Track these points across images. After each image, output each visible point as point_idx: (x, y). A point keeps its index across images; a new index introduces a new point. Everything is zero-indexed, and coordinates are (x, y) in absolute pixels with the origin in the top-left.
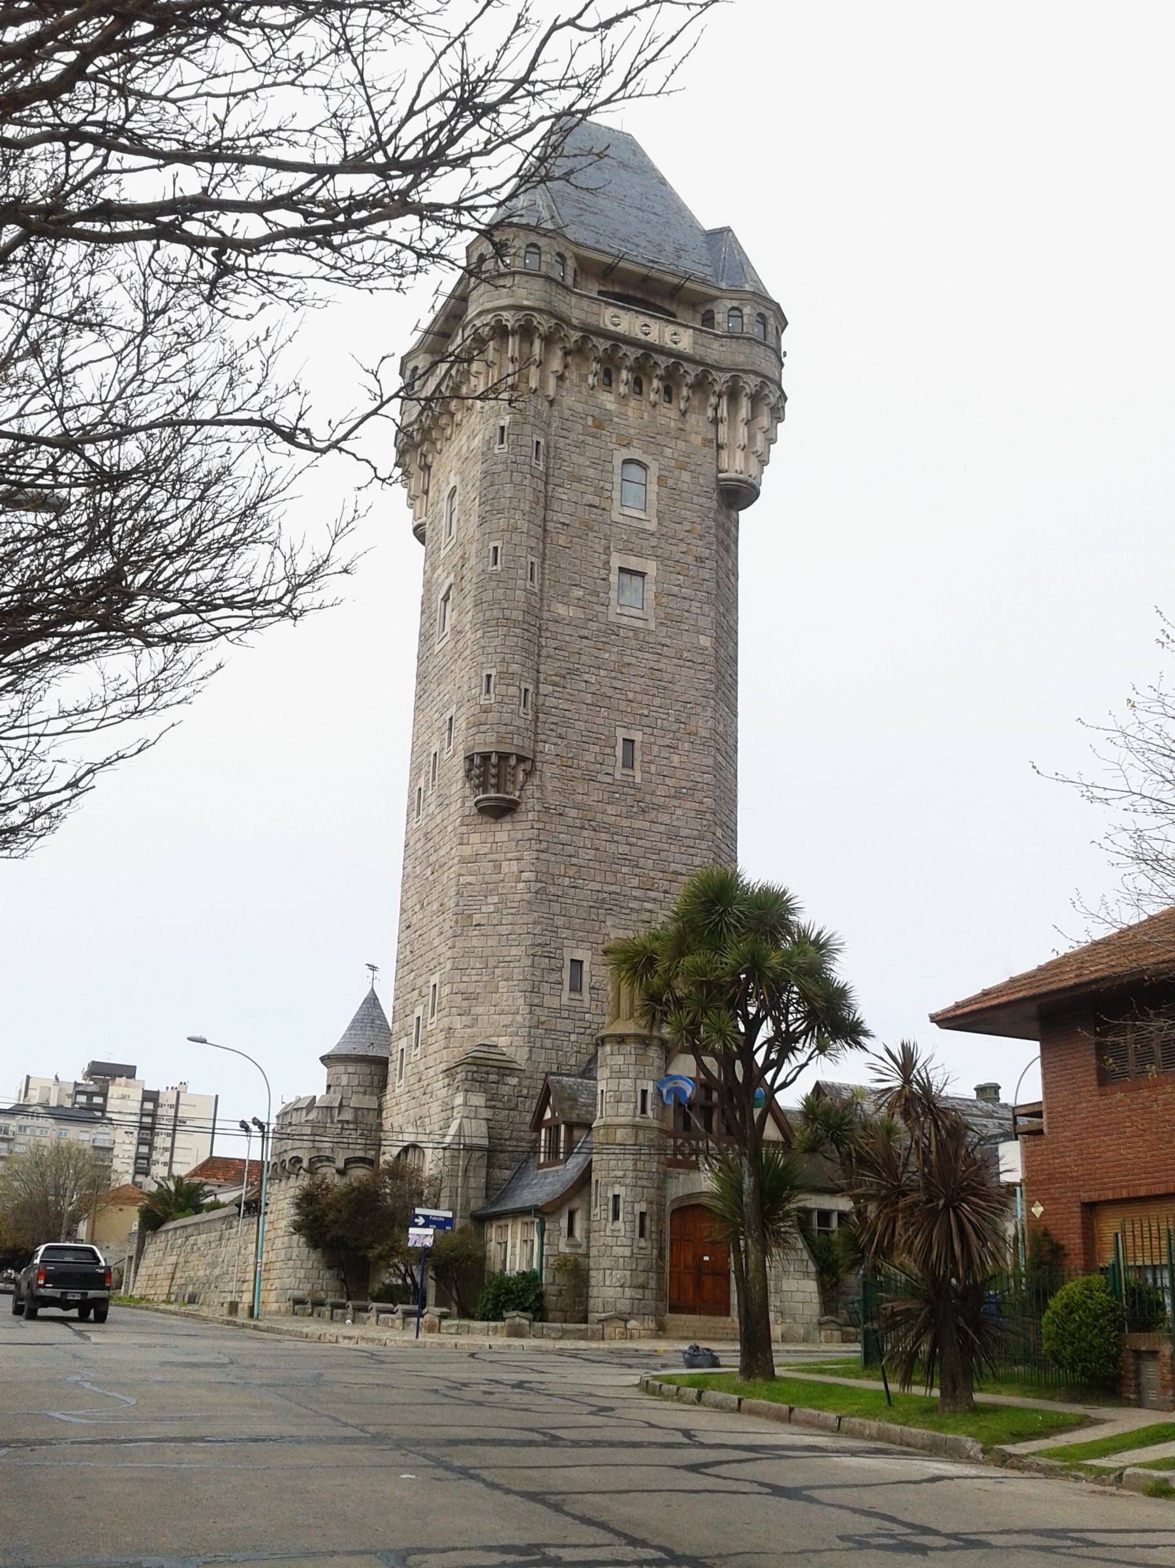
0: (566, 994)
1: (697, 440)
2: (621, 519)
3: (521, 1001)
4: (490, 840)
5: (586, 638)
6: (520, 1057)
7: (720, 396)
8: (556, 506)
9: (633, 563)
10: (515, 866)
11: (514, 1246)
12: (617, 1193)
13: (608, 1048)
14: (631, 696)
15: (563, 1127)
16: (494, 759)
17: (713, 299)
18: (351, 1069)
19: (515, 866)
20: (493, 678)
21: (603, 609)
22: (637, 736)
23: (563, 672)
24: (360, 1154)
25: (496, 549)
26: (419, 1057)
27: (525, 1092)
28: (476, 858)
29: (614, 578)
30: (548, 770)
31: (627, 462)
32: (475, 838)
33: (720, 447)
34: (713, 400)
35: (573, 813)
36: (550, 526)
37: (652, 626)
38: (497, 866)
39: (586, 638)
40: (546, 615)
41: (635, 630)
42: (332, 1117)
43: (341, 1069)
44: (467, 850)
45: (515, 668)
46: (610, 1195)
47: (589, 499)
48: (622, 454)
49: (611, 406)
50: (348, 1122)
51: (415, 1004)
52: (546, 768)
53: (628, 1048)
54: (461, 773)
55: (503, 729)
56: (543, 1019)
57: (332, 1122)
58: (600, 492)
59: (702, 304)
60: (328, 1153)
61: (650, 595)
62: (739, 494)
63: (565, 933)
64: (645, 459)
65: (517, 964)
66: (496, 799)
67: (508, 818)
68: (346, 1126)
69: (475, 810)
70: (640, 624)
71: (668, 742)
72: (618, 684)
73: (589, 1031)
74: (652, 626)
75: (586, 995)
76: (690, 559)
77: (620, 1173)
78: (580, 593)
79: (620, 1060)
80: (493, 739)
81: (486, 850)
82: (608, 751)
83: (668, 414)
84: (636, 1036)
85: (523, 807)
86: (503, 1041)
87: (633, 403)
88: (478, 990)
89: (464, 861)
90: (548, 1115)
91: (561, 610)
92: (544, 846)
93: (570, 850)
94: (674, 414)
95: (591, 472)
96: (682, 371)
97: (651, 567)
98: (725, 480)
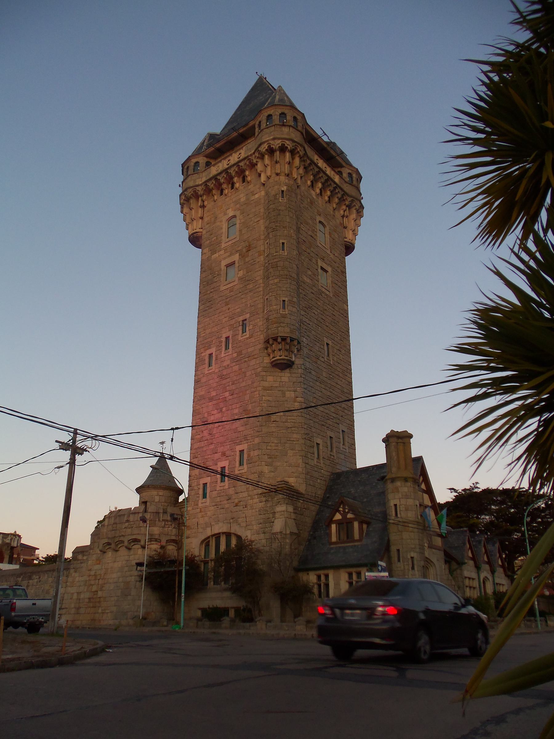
0: (316, 460)
1: (338, 221)
2: (320, 245)
4: (279, 380)
6: (302, 489)
7: (347, 206)
8: (301, 231)
9: (325, 266)
10: (293, 394)
12: (412, 556)
13: (398, 484)
15: (356, 524)
16: (288, 340)
17: (342, 166)
18: (161, 493)
19: (293, 394)
20: (286, 302)
21: (316, 282)
22: (330, 343)
24: (174, 538)
26: (227, 487)
28: (270, 388)
29: (319, 270)
30: (305, 351)
31: (320, 222)
32: (270, 378)
33: (345, 228)
34: (344, 207)
35: (313, 373)
37: (331, 295)
38: (284, 393)
40: (301, 279)
41: (327, 295)
43: (154, 492)
44: (266, 384)
45: (295, 300)
46: (409, 557)
48: (319, 218)
49: (315, 197)
50: (167, 521)
51: (218, 460)
52: (304, 349)
53: (409, 484)
54: (261, 346)
57: (159, 520)
58: (313, 231)
60: (157, 537)
61: (329, 281)
62: (349, 249)
66: (287, 360)
67: (288, 370)
68: (166, 523)
69: (269, 365)
70: (328, 293)
71: (338, 348)
72: (324, 318)
73: (323, 479)
74: (331, 295)
75: (322, 461)
76: (340, 271)
77: (413, 546)
78: (310, 273)
79: (406, 489)
80: (288, 330)
81: (277, 384)
82: (322, 347)
83: (330, 208)
84: (413, 478)
85: (295, 366)
86: (292, 481)
87: (320, 198)
88: (277, 454)
89: (265, 389)
90: (338, 517)
91: (305, 279)
92: (306, 386)
93: (313, 390)
94: (332, 209)
95: (310, 222)
97: (329, 269)
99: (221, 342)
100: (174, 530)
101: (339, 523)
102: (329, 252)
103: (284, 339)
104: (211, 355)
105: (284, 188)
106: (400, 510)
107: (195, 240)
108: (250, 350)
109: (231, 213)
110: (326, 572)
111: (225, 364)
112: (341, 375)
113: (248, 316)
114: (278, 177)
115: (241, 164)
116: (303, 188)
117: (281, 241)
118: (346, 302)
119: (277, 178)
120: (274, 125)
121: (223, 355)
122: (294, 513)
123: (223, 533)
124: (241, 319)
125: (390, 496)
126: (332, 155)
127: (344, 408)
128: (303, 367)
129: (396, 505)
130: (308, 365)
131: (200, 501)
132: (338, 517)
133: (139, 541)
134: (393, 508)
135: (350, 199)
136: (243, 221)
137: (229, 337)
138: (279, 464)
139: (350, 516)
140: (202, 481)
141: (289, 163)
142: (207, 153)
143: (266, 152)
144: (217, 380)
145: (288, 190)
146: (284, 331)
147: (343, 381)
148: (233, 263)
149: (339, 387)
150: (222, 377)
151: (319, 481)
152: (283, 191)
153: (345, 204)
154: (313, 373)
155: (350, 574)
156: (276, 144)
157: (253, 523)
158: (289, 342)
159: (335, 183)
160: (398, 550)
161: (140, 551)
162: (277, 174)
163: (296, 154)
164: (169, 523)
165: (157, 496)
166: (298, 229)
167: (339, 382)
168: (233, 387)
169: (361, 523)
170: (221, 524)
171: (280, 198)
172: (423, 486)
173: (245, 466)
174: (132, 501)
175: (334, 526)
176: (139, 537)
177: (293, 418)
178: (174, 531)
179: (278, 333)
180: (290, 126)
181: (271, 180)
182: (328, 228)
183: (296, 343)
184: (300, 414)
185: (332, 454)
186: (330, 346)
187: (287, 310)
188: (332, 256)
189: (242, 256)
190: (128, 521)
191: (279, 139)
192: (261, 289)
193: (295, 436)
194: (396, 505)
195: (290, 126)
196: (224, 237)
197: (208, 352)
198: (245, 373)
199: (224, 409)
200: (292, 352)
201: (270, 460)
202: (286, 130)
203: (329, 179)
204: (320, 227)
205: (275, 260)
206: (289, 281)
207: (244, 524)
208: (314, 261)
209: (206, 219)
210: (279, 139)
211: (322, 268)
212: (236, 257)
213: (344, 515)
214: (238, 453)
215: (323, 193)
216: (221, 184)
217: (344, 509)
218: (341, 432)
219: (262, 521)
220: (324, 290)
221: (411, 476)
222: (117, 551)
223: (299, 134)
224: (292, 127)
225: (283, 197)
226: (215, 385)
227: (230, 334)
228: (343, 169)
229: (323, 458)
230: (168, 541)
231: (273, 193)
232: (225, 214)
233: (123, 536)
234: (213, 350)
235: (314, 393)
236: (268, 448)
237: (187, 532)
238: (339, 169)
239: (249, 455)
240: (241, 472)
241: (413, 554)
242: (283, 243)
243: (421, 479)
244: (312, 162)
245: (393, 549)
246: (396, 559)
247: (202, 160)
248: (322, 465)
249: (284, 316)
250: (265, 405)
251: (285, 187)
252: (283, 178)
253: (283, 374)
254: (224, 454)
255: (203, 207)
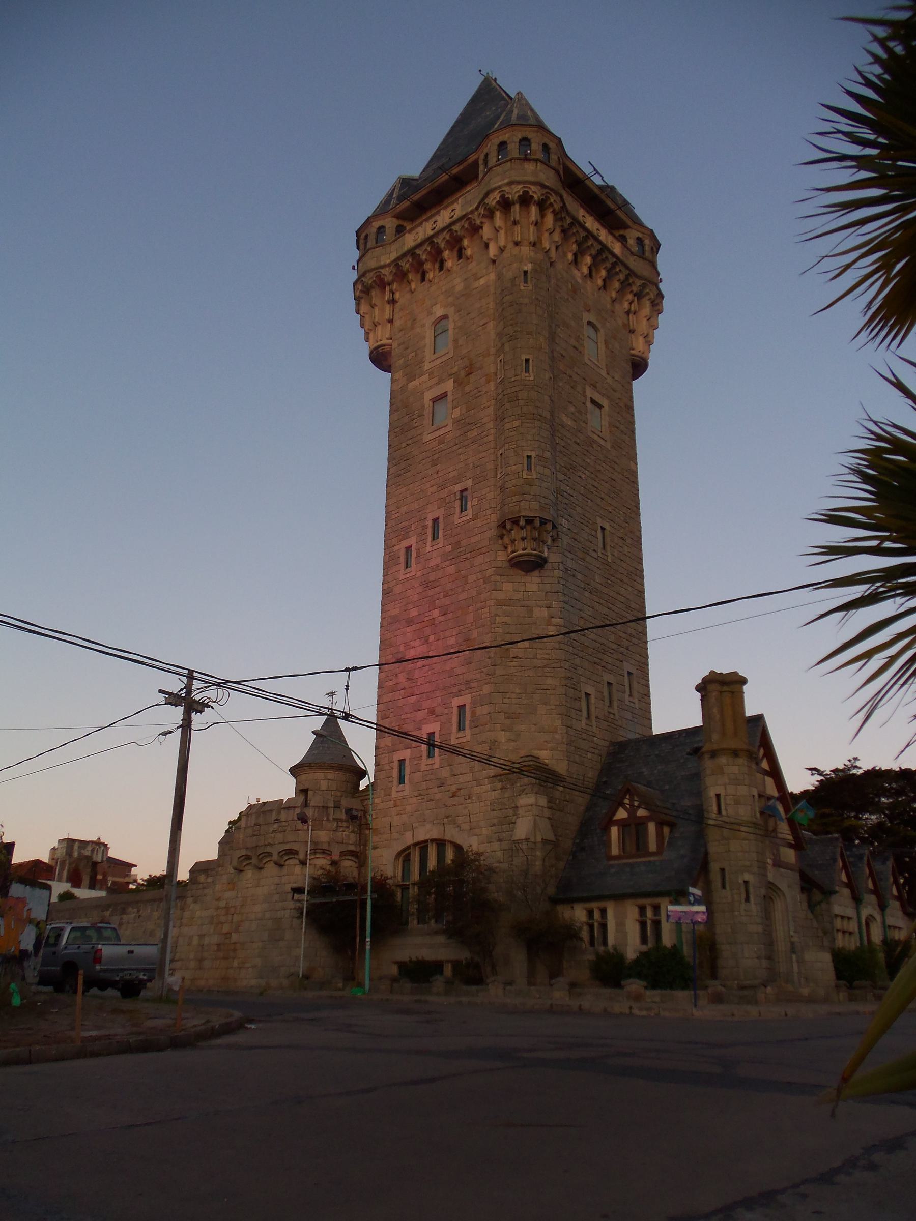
0: (584, 722)
1: (620, 322)
2: (589, 363)
3: (558, 723)
5: (578, 444)
6: (561, 768)
7: (635, 295)
10: (545, 613)
11: (620, 925)
12: (746, 879)
13: (723, 760)
14: (602, 496)
15: (652, 827)
17: (626, 227)
19: (545, 613)
20: (533, 459)
21: (584, 425)
23: (569, 466)
24: (352, 848)
25: (527, 361)
26: (437, 766)
27: (568, 797)
29: (589, 404)
30: (565, 540)
31: (589, 323)
32: (507, 586)
33: (632, 331)
35: (579, 576)
36: (555, 354)
37: (608, 446)
38: (530, 610)
39: (578, 444)
41: (600, 446)
42: (328, 815)
43: (320, 775)
44: (501, 596)
46: (741, 881)
47: (572, 342)
48: (586, 317)
49: (580, 281)
50: (341, 820)
52: (564, 537)
53: (741, 761)
54: (493, 532)
55: (543, 500)
56: (573, 738)
57: (328, 820)
58: (578, 339)
59: (618, 228)
60: (325, 847)
61: (605, 423)
62: (639, 367)
63: (580, 671)
64: (599, 325)
65: (553, 692)
66: (535, 555)
67: (536, 573)
69: (506, 564)
70: (602, 442)
72: (596, 484)
73: (597, 751)
74: (608, 446)
75: (594, 724)
77: (747, 863)
78: (572, 409)
79: (735, 769)
80: (537, 507)
81: (519, 596)
84: (748, 751)
85: (548, 566)
86: (544, 755)
87: (589, 282)
89: (500, 603)
90: (622, 814)
91: (565, 419)
92: (566, 599)
94: (608, 299)
96: (618, 270)
97: (605, 403)
98: (633, 355)
99: (425, 527)
100: (353, 835)
101: (623, 824)
102: (604, 373)
103: (530, 521)
104: (408, 549)
105: (528, 267)
106: (726, 804)
107: (380, 358)
108: (473, 540)
109: (439, 312)
110: (602, 904)
111: (432, 563)
112: (626, 580)
113: (469, 483)
114: (517, 248)
115: (456, 228)
116: (559, 266)
117: (524, 357)
118: (633, 458)
119: (516, 250)
120: (511, 160)
121: (428, 549)
122: (549, 808)
123: (433, 840)
124: (458, 488)
125: (709, 781)
126: (608, 208)
127: (630, 635)
128: (562, 567)
129: (718, 796)
130: (569, 563)
131: (394, 789)
132: (622, 814)
133: (297, 853)
134: (714, 800)
135: (639, 283)
136: (459, 324)
137: (438, 518)
138: (523, 727)
139: (641, 812)
140: (397, 756)
141: (536, 224)
142: (398, 210)
143: (497, 207)
144: (420, 590)
145: (535, 270)
146: (529, 508)
147: (630, 589)
148: (444, 396)
149: (623, 600)
150: (427, 585)
151: (589, 755)
152: (526, 272)
153: (632, 292)
154: (579, 576)
155: (642, 909)
156: (514, 192)
157: (482, 823)
158: (538, 526)
159: (614, 255)
160: (723, 870)
161: (298, 869)
162: (517, 244)
163: (547, 208)
164: (345, 824)
165: (324, 780)
166: (552, 337)
167: (623, 591)
168: (447, 601)
169: (660, 825)
170: (428, 826)
171: (522, 284)
172: (765, 765)
173: (468, 732)
174: (284, 789)
175: (614, 830)
176: (295, 847)
177: (544, 651)
178: (353, 838)
179: (519, 511)
180: (536, 160)
181: (506, 254)
182: (602, 332)
183: (549, 527)
184: (557, 646)
185: (611, 710)
186: (607, 533)
187: (534, 472)
188: (609, 380)
189: (459, 383)
190: (277, 821)
191: (519, 183)
192: (491, 438)
193: (549, 681)
194: (718, 796)
195: (536, 160)
196: (428, 354)
197: (405, 544)
198: (465, 577)
199: (432, 638)
200: (544, 542)
201: (508, 722)
202: (530, 167)
203: (604, 248)
204: (588, 331)
205: (514, 389)
206: (537, 424)
207: (466, 826)
208: (579, 388)
209: (398, 323)
210: (519, 183)
211: (593, 402)
212: (449, 386)
213: (632, 811)
214: (455, 711)
215: (594, 274)
216: (421, 264)
217: (632, 800)
218: (626, 675)
219: (495, 821)
220: (596, 437)
221: (745, 747)
222: (261, 868)
223: (552, 173)
224: (542, 162)
225: (526, 282)
226: (416, 598)
227: (440, 513)
228: (628, 231)
229: (597, 717)
230: (343, 854)
231: (509, 275)
232: (430, 313)
233: (270, 844)
234: (412, 541)
235: (580, 610)
236: (506, 701)
237: (373, 839)
238: (622, 232)
239: (473, 714)
240: (460, 740)
241: (747, 877)
242: (527, 361)
243: (762, 751)
244: (576, 222)
245: (714, 867)
246: (719, 884)
247: (390, 223)
248: (595, 729)
249: (529, 483)
250: (500, 630)
251: (530, 265)
252: (526, 250)
253: (528, 579)
254: (432, 712)
255: (393, 302)
